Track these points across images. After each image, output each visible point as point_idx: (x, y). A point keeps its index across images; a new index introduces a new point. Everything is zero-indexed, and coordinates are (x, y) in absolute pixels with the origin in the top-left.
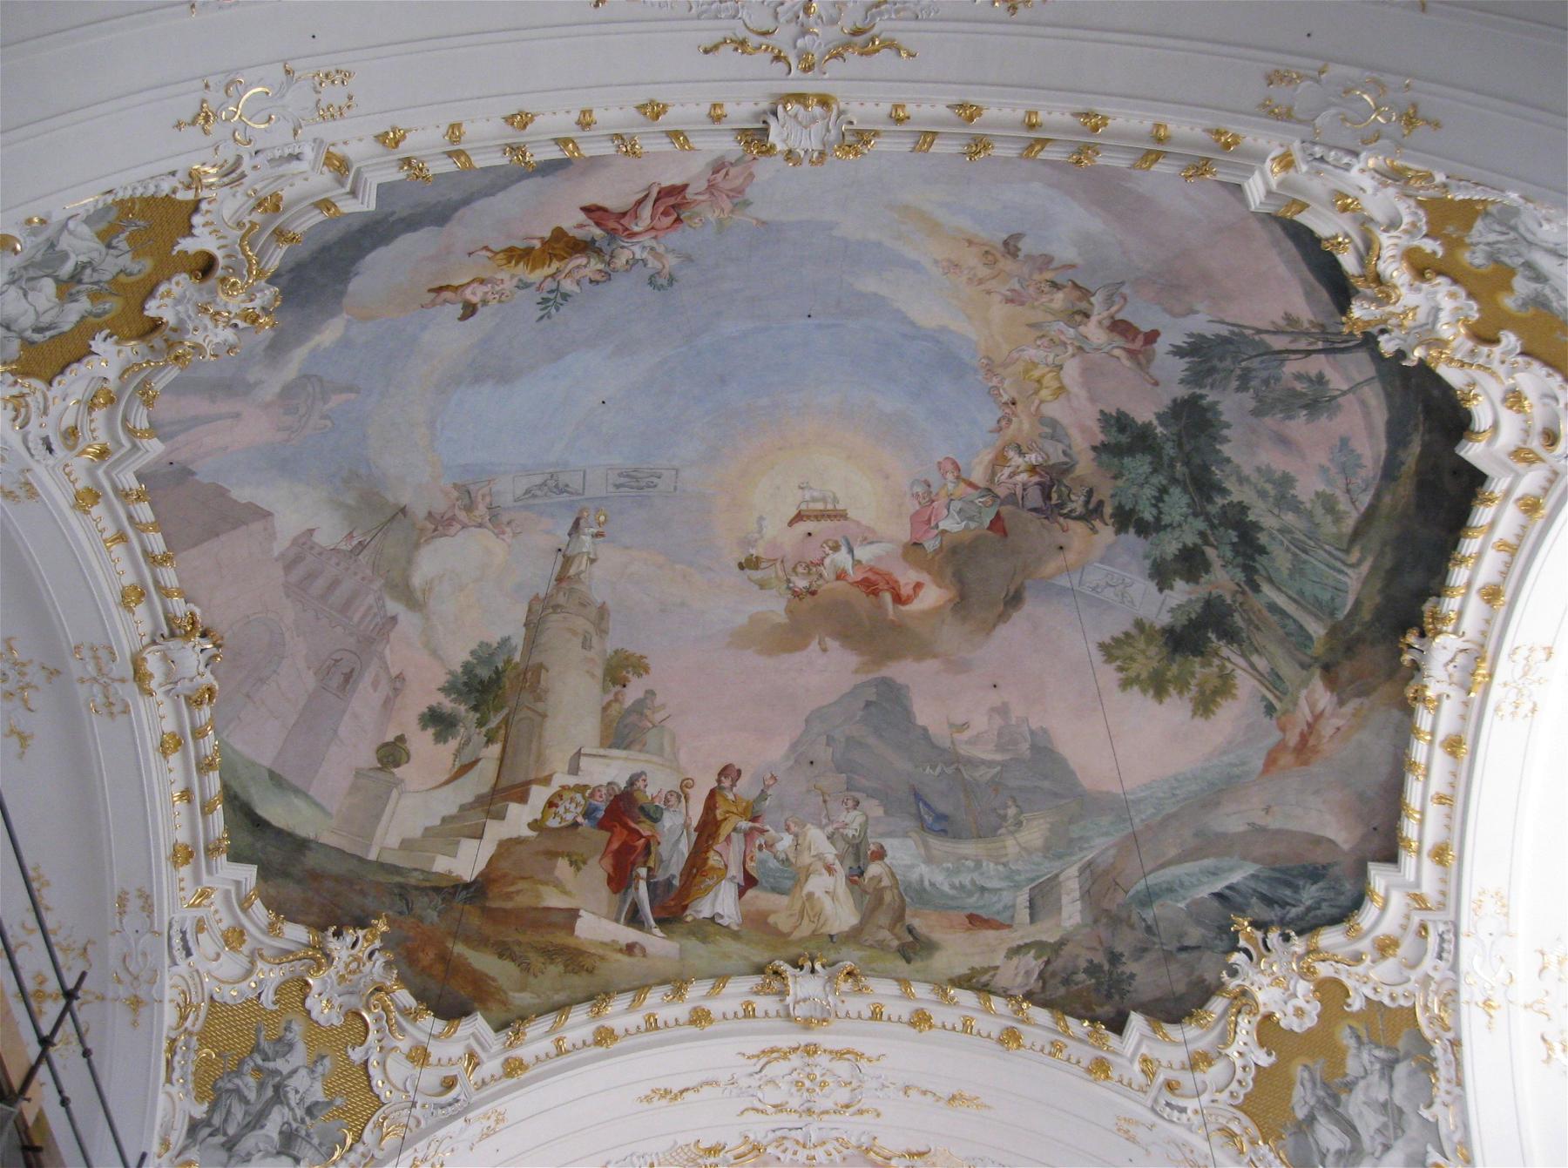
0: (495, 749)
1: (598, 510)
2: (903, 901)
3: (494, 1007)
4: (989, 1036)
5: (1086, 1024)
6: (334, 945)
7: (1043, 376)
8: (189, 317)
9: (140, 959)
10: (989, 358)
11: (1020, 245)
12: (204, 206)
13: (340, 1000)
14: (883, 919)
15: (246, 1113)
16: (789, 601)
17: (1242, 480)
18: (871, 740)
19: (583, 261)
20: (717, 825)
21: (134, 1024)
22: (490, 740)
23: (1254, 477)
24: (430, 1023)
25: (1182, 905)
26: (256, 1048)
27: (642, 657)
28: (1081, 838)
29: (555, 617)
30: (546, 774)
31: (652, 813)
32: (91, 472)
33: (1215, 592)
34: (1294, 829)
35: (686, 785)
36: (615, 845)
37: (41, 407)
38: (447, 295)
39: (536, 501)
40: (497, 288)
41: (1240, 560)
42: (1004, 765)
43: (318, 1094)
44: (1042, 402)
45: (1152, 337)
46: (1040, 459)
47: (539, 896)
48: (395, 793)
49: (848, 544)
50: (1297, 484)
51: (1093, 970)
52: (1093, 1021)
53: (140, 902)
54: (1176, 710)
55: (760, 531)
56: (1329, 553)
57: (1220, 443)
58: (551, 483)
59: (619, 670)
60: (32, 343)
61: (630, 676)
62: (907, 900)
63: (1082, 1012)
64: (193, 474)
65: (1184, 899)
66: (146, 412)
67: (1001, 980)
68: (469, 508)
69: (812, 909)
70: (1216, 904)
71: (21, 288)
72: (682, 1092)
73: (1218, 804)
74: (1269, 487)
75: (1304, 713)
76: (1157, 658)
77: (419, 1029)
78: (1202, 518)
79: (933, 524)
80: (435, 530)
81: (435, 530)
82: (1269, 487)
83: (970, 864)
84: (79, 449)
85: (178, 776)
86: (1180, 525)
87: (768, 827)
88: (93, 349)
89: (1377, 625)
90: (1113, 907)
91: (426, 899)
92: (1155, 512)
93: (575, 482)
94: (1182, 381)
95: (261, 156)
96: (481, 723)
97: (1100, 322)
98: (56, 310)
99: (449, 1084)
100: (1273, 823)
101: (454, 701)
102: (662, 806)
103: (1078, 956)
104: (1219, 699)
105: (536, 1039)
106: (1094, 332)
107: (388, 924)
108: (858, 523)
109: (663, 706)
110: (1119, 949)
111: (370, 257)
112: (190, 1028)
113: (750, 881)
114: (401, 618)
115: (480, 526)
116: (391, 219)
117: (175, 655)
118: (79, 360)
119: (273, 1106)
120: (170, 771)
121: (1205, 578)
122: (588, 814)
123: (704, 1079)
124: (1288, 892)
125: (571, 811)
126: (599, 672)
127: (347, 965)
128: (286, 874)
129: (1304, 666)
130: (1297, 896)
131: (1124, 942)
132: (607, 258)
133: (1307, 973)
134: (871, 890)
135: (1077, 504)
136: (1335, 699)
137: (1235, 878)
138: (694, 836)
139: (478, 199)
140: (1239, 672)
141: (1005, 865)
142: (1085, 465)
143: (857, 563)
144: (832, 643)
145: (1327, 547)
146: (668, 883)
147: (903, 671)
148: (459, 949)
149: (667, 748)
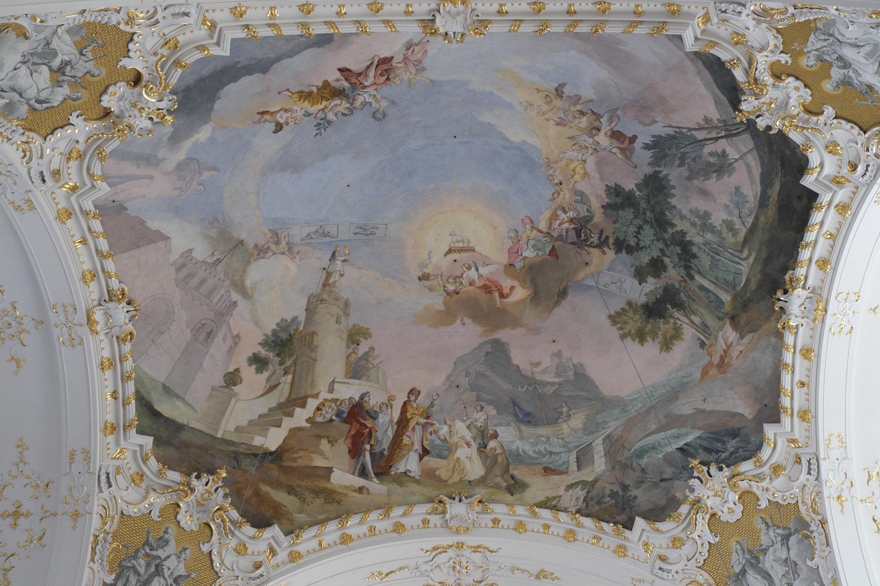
0: (289, 378)
1: (345, 247)
2: (507, 460)
3: (284, 521)
4: (558, 535)
5: (612, 525)
6: (194, 482)
7: (576, 167)
8: (126, 109)
9: (80, 489)
10: (548, 158)
11: (564, 91)
12: (135, 37)
13: (197, 516)
14: (497, 471)
15: (138, 581)
16: (445, 297)
17: (682, 218)
18: (489, 373)
19: (338, 102)
20: (408, 421)
21: (74, 528)
22: (286, 373)
23: (689, 215)
24: (249, 530)
25: (660, 456)
26: (147, 543)
27: (367, 329)
28: (603, 422)
29: (321, 306)
30: (316, 392)
31: (372, 415)
32: (68, 198)
33: (669, 283)
34: (720, 409)
35: (391, 399)
36: (353, 432)
37: (39, 152)
38: (267, 117)
39: (313, 241)
40: (294, 115)
41: (682, 263)
42: (560, 384)
43: (182, 571)
44: (575, 182)
45: (633, 139)
46: (575, 215)
47: (311, 460)
48: (233, 400)
49: (475, 265)
50: (712, 216)
51: (613, 495)
52: (615, 523)
53: (83, 456)
54: (651, 349)
55: (430, 258)
56: (731, 254)
57: (670, 198)
58: (320, 231)
59: (355, 336)
60: (35, 110)
61: (361, 339)
62: (510, 460)
63: (609, 519)
64: (126, 209)
65: (661, 452)
66: (100, 165)
67: (564, 503)
68: (277, 243)
69: (459, 467)
70: (679, 454)
71: (29, 68)
72: (387, 575)
73: (677, 399)
74: (697, 220)
75: (721, 345)
76: (640, 321)
77: (243, 533)
78: (662, 241)
79: (520, 253)
80: (259, 254)
81: (259, 254)
82: (697, 220)
83: (544, 439)
84: (61, 183)
85: (110, 383)
86: (650, 246)
87: (434, 422)
88: (71, 121)
89: (760, 291)
90: (623, 459)
91: (249, 460)
92: (636, 240)
93: (333, 230)
94: (649, 164)
95: (167, 11)
96: (281, 363)
97: (606, 133)
98: (50, 89)
99: (258, 566)
100: (708, 407)
101: (267, 350)
102: (378, 410)
103: (604, 488)
104: (674, 341)
105: (307, 540)
106: (603, 139)
107: (228, 472)
108: (481, 254)
109: (379, 355)
110: (627, 482)
111: (226, 88)
112: (108, 530)
113: (425, 452)
114: (238, 303)
115: (283, 253)
116: (238, 66)
117: (111, 312)
118: (62, 127)
119: (154, 577)
120: (106, 380)
121: (664, 275)
122: (339, 414)
123: (401, 565)
124: (719, 445)
125: (329, 413)
126: (345, 337)
127: (202, 495)
128: (169, 444)
129: (720, 319)
130: (725, 447)
131: (630, 479)
132: (351, 100)
133: (734, 487)
134: (490, 455)
135: (595, 239)
136: (738, 335)
137: (689, 439)
138: (395, 427)
139: (283, 59)
140: (684, 325)
141: (562, 439)
142: (599, 217)
143: (480, 276)
144: (467, 321)
145: (730, 250)
146: (382, 452)
147: (503, 335)
148: (265, 488)
149: (381, 378)
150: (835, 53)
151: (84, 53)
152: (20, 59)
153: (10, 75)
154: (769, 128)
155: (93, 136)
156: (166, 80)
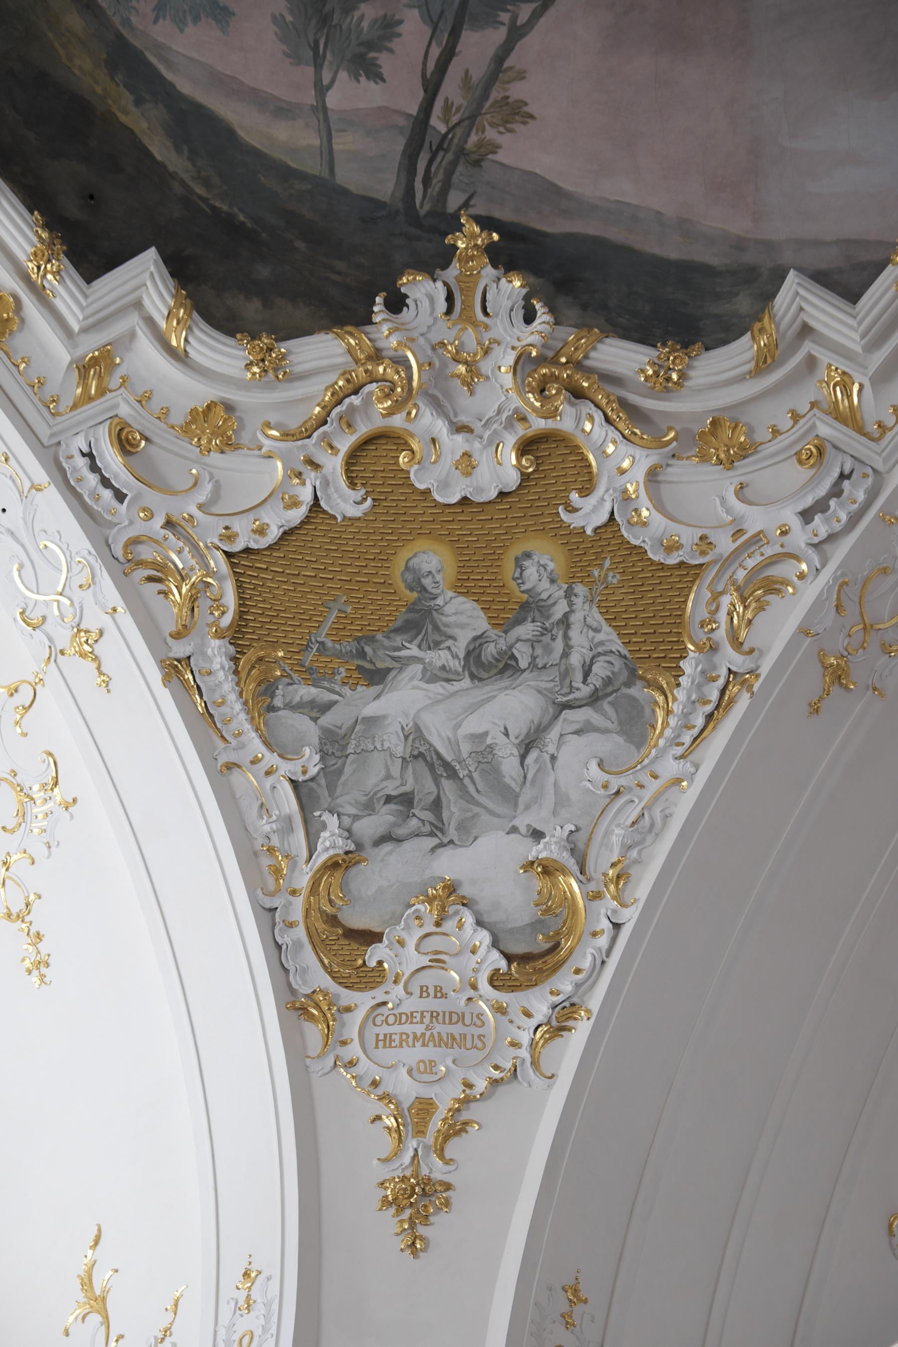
150: (533, 665)
154: (397, 304)
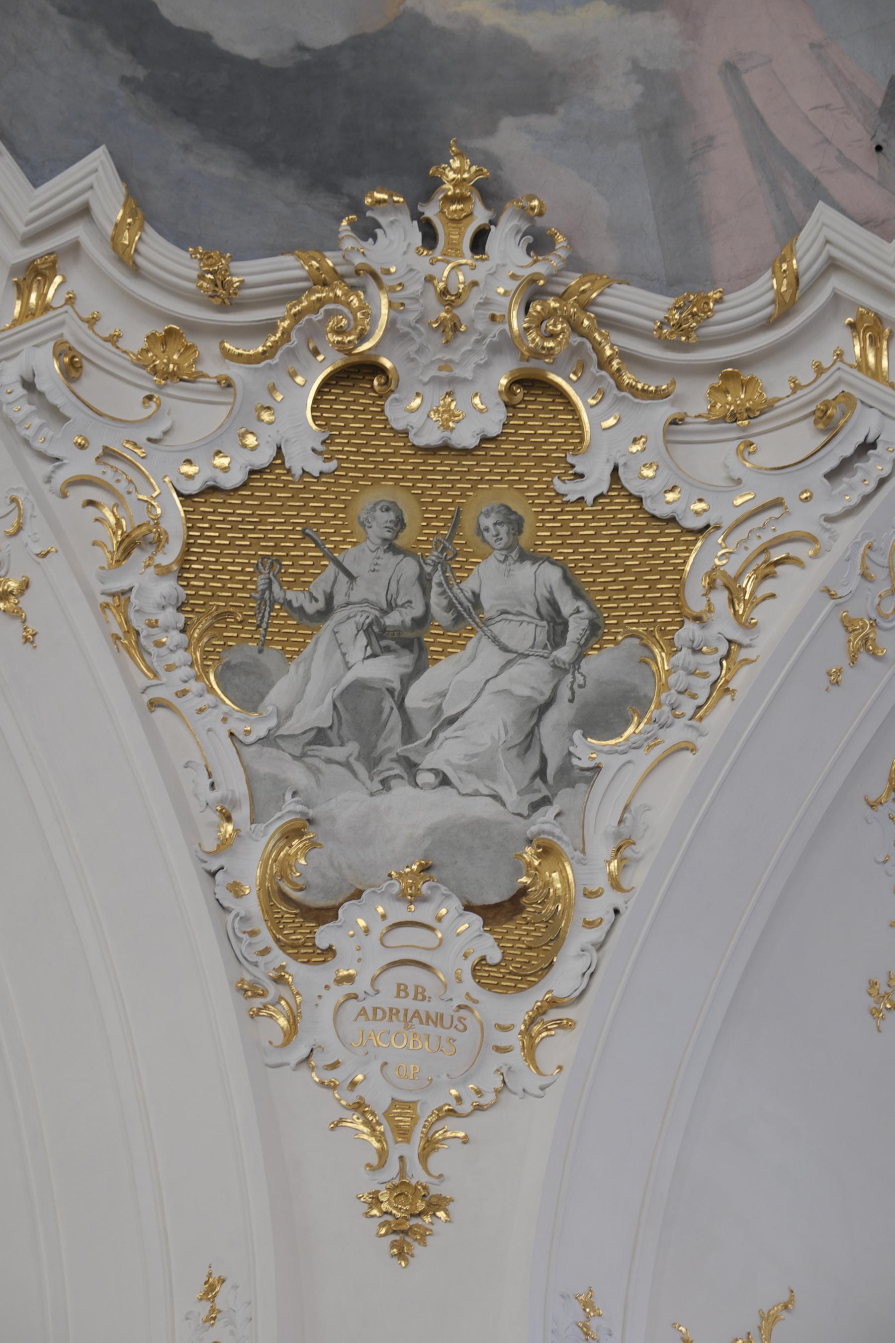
60: (595, 629)
98: (496, 628)
111: (250, 52)
116: (141, 73)
151: (321, 605)
152: (401, 791)
153: (472, 783)
155: (632, 389)
156: (296, 295)
